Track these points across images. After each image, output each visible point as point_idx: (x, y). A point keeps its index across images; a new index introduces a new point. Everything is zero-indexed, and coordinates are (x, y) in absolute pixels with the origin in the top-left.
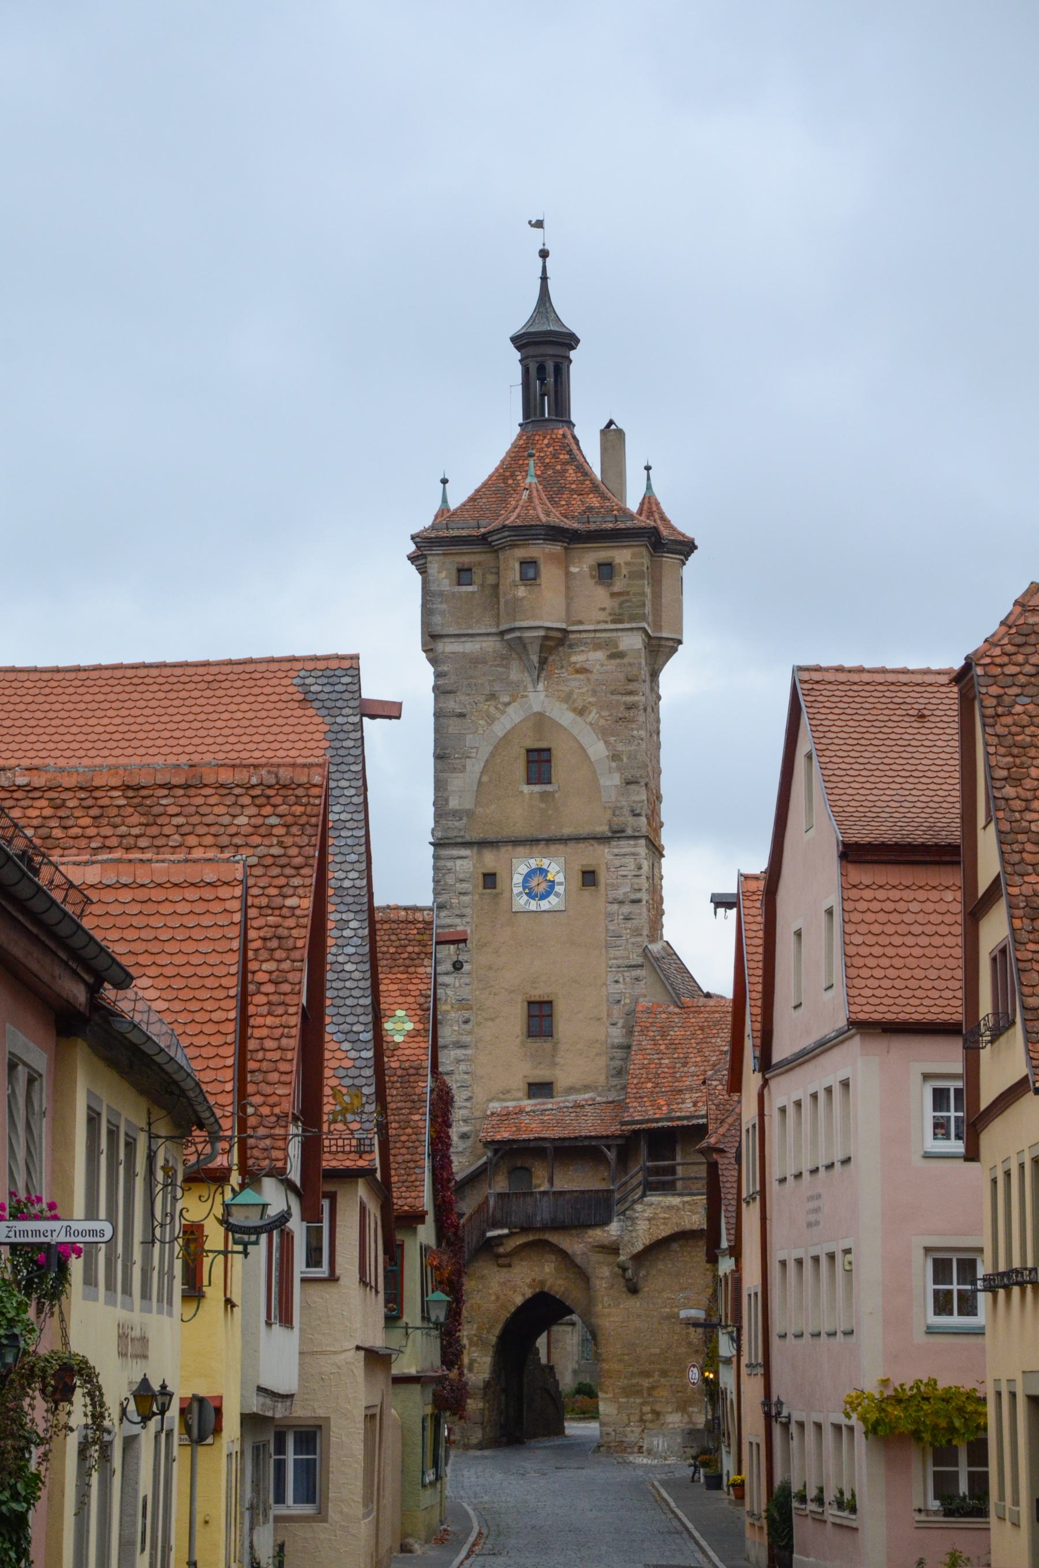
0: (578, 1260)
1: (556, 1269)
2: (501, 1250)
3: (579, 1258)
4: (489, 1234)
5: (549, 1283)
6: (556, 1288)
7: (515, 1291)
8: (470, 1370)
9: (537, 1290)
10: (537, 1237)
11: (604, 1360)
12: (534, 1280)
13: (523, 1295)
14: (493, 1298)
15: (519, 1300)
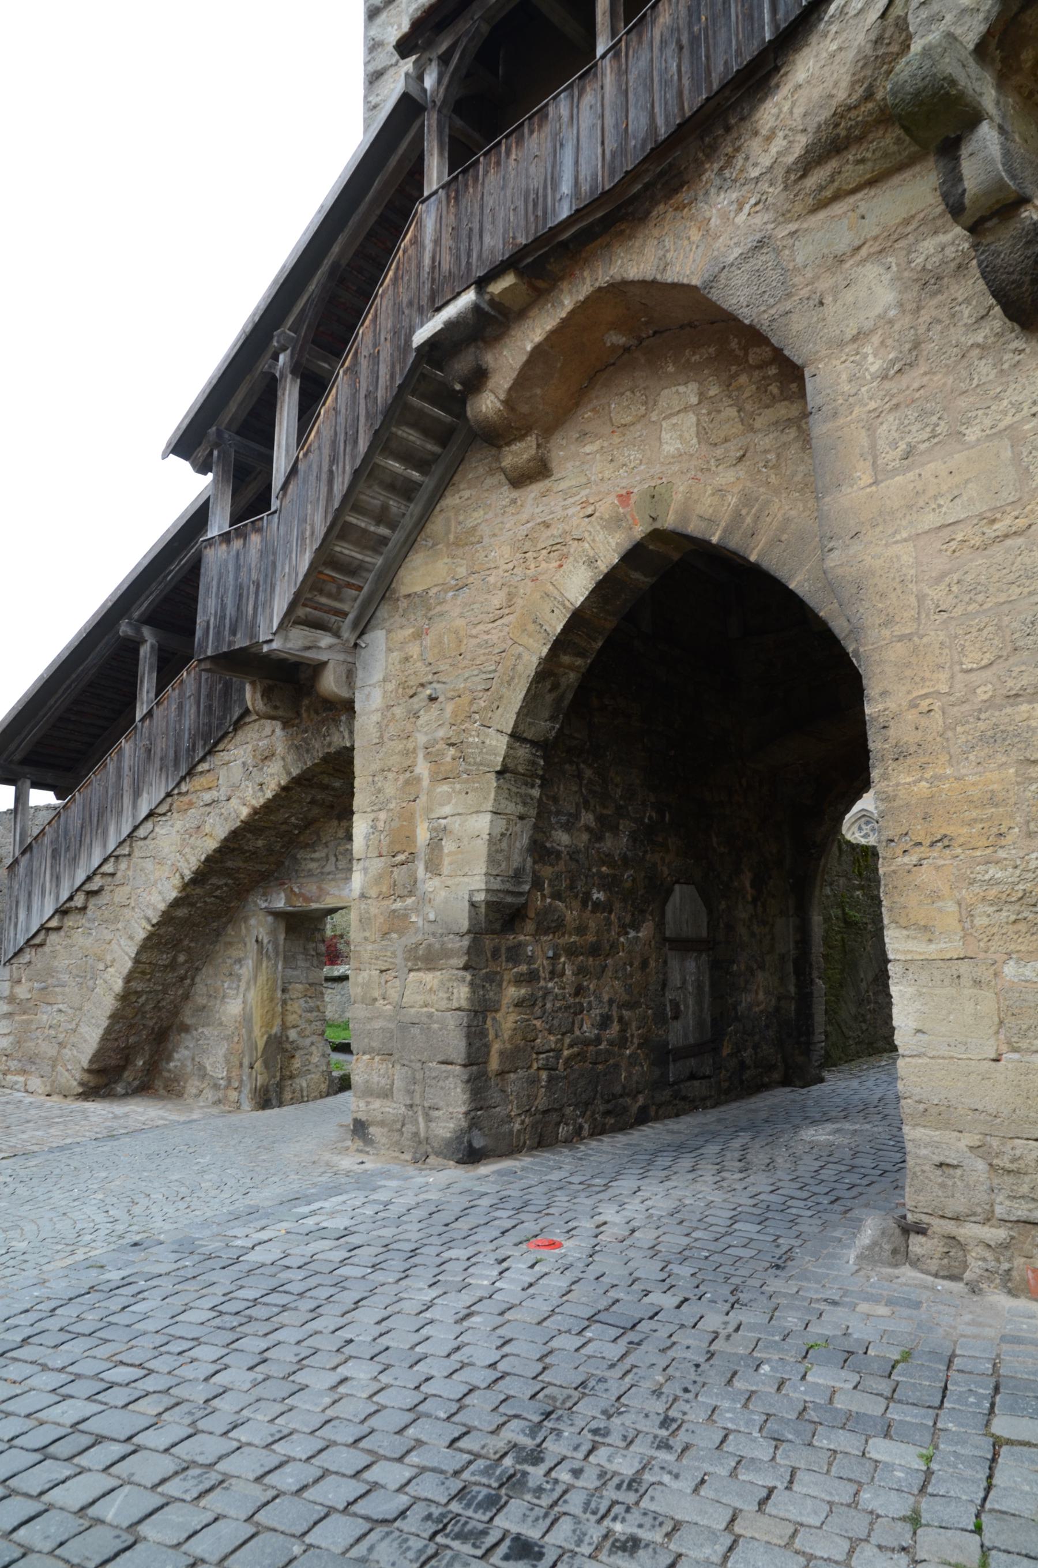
0: (739, 297)
1: (702, 434)
2: (488, 404)
3: (739, 278)
4: (421, 335)
5: (678, 498)
6: (706, 505)
7: (566, 556)
8: (434, 867)
9: (639, 531)
10: (584, 290)
11: (900, 755)
12: (624, 498)
13: (591, 562)
14: (498, 599)
15: (576, 586)
